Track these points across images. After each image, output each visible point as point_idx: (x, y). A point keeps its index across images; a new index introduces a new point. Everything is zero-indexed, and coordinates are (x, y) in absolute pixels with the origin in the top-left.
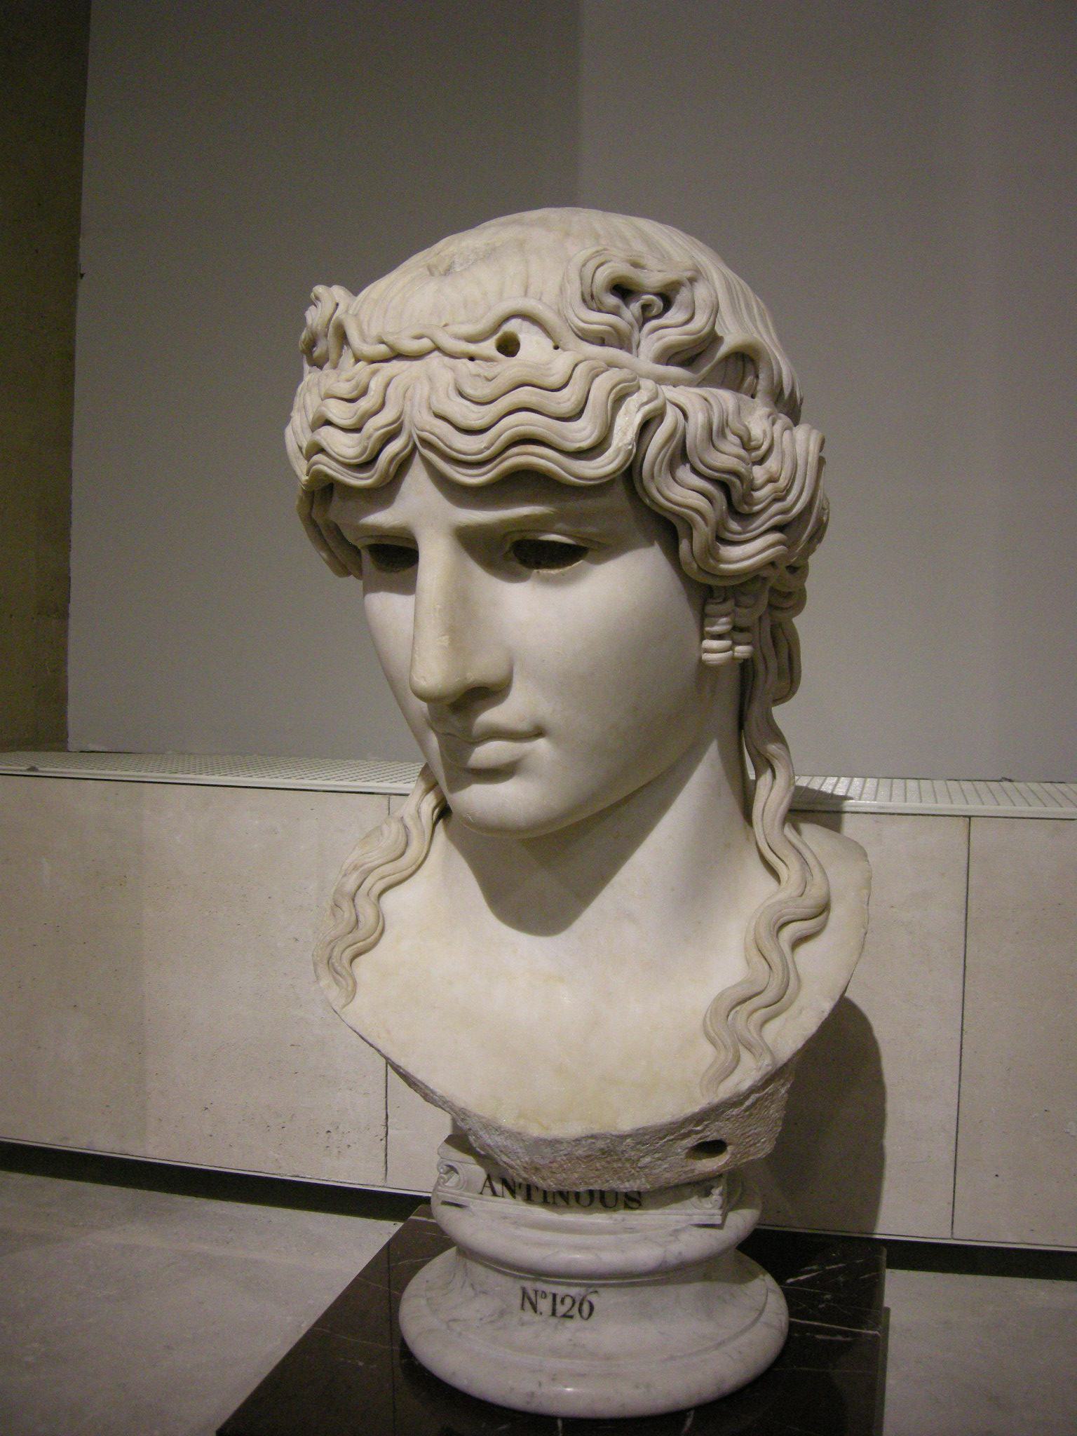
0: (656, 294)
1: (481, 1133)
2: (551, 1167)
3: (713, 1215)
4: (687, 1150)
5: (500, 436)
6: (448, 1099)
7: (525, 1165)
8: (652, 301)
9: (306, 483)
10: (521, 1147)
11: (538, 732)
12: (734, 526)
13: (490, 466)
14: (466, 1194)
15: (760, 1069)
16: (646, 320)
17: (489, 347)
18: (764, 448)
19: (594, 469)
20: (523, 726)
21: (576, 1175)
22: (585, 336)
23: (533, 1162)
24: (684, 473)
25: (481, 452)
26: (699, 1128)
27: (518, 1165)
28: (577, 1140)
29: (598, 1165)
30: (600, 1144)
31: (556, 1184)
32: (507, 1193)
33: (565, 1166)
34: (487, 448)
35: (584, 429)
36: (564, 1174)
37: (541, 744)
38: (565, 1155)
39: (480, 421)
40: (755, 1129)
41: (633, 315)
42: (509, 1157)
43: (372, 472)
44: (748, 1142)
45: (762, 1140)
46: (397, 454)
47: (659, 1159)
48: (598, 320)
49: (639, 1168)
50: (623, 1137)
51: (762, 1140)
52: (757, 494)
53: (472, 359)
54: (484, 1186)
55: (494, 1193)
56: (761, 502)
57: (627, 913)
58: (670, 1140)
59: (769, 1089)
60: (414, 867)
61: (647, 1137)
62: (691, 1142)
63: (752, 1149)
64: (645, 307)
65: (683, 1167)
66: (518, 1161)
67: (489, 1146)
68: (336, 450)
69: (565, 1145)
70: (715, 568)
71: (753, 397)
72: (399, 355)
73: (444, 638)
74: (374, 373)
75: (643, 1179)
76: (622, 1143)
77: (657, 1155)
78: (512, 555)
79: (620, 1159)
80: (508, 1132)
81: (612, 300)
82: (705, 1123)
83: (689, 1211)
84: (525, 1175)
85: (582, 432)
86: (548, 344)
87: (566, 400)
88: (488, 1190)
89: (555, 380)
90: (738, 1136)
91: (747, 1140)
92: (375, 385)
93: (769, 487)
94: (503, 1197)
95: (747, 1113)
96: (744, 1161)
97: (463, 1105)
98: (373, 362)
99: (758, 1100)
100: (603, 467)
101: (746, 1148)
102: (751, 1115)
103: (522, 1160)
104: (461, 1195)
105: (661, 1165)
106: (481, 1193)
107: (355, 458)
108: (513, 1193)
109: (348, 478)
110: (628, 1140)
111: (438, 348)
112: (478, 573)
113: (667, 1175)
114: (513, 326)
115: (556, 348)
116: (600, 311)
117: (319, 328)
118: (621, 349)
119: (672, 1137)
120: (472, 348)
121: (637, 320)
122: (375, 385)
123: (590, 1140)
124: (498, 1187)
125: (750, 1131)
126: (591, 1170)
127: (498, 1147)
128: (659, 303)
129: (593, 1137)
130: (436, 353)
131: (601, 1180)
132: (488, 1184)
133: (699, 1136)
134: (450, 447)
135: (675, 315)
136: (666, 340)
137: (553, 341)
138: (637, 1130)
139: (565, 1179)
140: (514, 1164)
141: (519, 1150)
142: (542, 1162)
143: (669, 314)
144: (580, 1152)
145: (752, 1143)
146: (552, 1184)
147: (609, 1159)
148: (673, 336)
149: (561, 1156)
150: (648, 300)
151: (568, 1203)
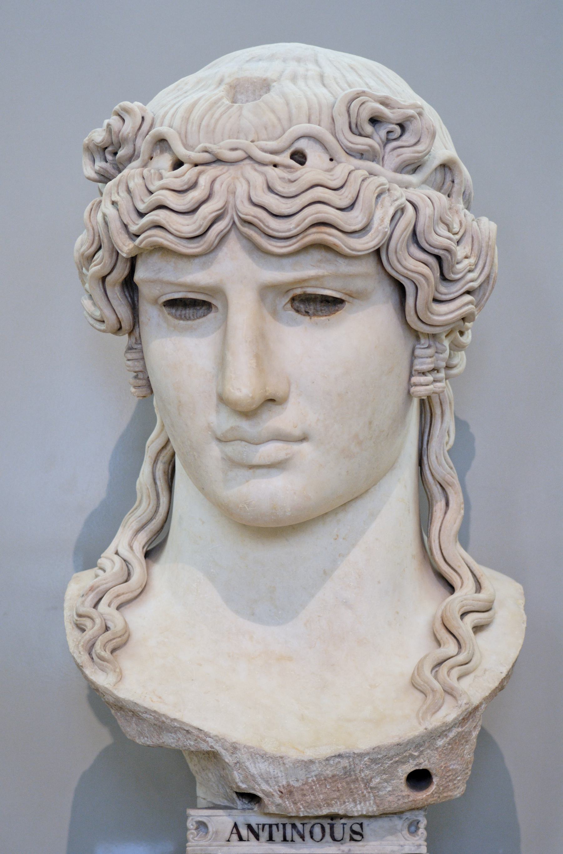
1: (247, 764)
2: (302, 790)
3: (420, 845)
5: (305, 220)
6: (220, 737)
7: (282, 790)
8: (395, 128)
9: (128, 251)
10: (281, 771)
11: (304, 439)
12: (443, 289)
13: (294, 240)
14: (215, 843)
16: (388, 141)
17: (284, 158)
18: (461, 234)
19: (364, 244)
20: (297, 432)
21: (321, 796)
22: (350, 153)
23: (289, 785)
24: (414, 250)
25: (289, 230)
26: (416, 754)
27: (275, 791)
28: (327, 760)
29: (340, 785)
30: (345, 763)
31: (304, 807)
32: (251, 836)
33: (314, 787)
34: (295, 228)
35: (357, 217)
36: (312, 797)
37: (305, 446)
38: (316, 776)
39: (289, 210)
40: (454, 765)
41: (381, 139)
42: (269, 784)
43: (202, 243)
44: (448, 776)
45: (458, 778)
46: (222, 231)
47: (386, 781)
48: (361, 143)
49: (371, 788)
50: (361, 755)
51: (458, 778)
52: (459, 267)
53: (275, 166)
54: (232, 833)
55: (241, 839)
56: (461, 272)
57: (344, 601)
58: (396, 762)
59: (466, 728)
60: (140, 590)
61: (379, 756)
62: (410, 768)
63: (451, 784)
65: (401, 791)
66: (276, 787)
67: (253, 776)
68: (175, 227)
69: (317, 765)
70: (430, 318)
71: (449, 196)
72: (218, 161)
74: (200, 173)
75: (372, 802)
76: (360, 761)
77: (384, 777)
78: (289, 306)
79: (357, 779)
80: (272, 758)
81: (369, 129)
82: (421, 749)
83: (402, 843)
84: (279, 801)
86: (327, 158)
88: (235, 837)
89: (336, 183)
90: (442, 768)
91: (448, 774)
92: (204, 181)
93: (466, 262)
94: (248, 840)
95: (450, 747)
96: (445, 795)
97: (234, 740)
98: (196, 165)
100: (367, 243)
101: (447, 782)
102: (452, 749)
103: (280, 785)
104: (210, 846)
105: (386, 787)
106: (229, 841)
107: (190, 233)
108: (257, 837)
109: (179, 247)
110: (366, 759)
111: (250, 157)
112: (269, 318)
113: (390, 798)
114: (302, 145)
115: (331, 160)
116: (360, 135)
117: (130, 135)
118: (373, 162)
119: (397, 759)
120: (277, 159)
121: (383, 142)
122: (204, 181)
123: (337, 760)
124: (244, 832)
126: (334, 791)
127: (261, 775)
129: (340, 756)
130: (247, 161)
131: (340, 802)
132: (235, 831)
133: (415, 763)
134: (268, 227)
135: (407, 139)
136: (403, 156)
137: (330, 155)
138: (374, 749)
139: (312, 801)
140: (272, 791)
141: (280, 775)
142: (296, 785)
143: (404, 138)
144: (329, 772)
145: (450, 778)
146: (301, 807)
147: (348, 779)
148: (408, 154)
149: (312, 777)
150: (392, 128)
151: (304, 840)
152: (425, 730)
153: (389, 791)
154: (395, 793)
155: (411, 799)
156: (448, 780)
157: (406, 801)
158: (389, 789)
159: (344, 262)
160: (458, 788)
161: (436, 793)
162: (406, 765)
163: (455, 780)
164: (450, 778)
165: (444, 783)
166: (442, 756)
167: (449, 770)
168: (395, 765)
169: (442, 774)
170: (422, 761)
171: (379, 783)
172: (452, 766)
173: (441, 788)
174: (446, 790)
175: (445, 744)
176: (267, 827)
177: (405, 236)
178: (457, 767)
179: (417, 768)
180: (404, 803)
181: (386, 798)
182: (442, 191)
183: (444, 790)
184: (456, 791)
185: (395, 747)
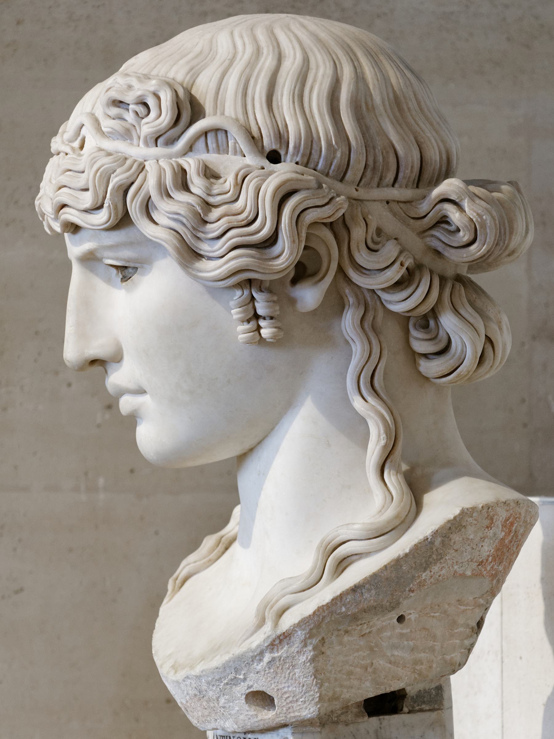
0: (137, 104)
4: (244, 696)
11: (141, 391)
15: (265, 633)
40: (288, 687)
45: (301, 700)
51: (301, 700)
52: (209, 226)
58: (227, 684)
59: (282, 652)
62: (241, 690)
63: (295, 705)
64: (137, 113)
73: (72, 328)
85: (87, 199)
87: (81, 180)
90: (275, 690)
95: (272, 670)
96: (292, 715)
99: (273, 659)
119: (226, 681)
125: (284, 687)
128: (141, 110)
135: (153, 114)
145: (291, 699)
152: (232, 656)
153: (238, 711)
154: (243, 712)
155: (259, 718)
156: (288, 701)
157: (256, 720)
158: (237, 708)
159: (105, 235)
160: (306, 708)
161: (280, 713)
162: (240, 687)
163: (297, 701)
164: (291, 699)
165: (284, 704)
166: (269, 679)
167: (285, 693)
168: (228, 687)
169: (278, 695)
170: (251, 683)
171: (225, 703)
172: (287, 688)
173: (284, 709)
174: (291, 710)
175: (265, 668)
176: (222, 737)
177: (136, 207)
178: (294, 689)
179: (252, 690)
180: (255, 721)
181: (238, 716)
182: (230, 153)
183: (289, 711)
184: (305, 712)
185: (215, 671)
